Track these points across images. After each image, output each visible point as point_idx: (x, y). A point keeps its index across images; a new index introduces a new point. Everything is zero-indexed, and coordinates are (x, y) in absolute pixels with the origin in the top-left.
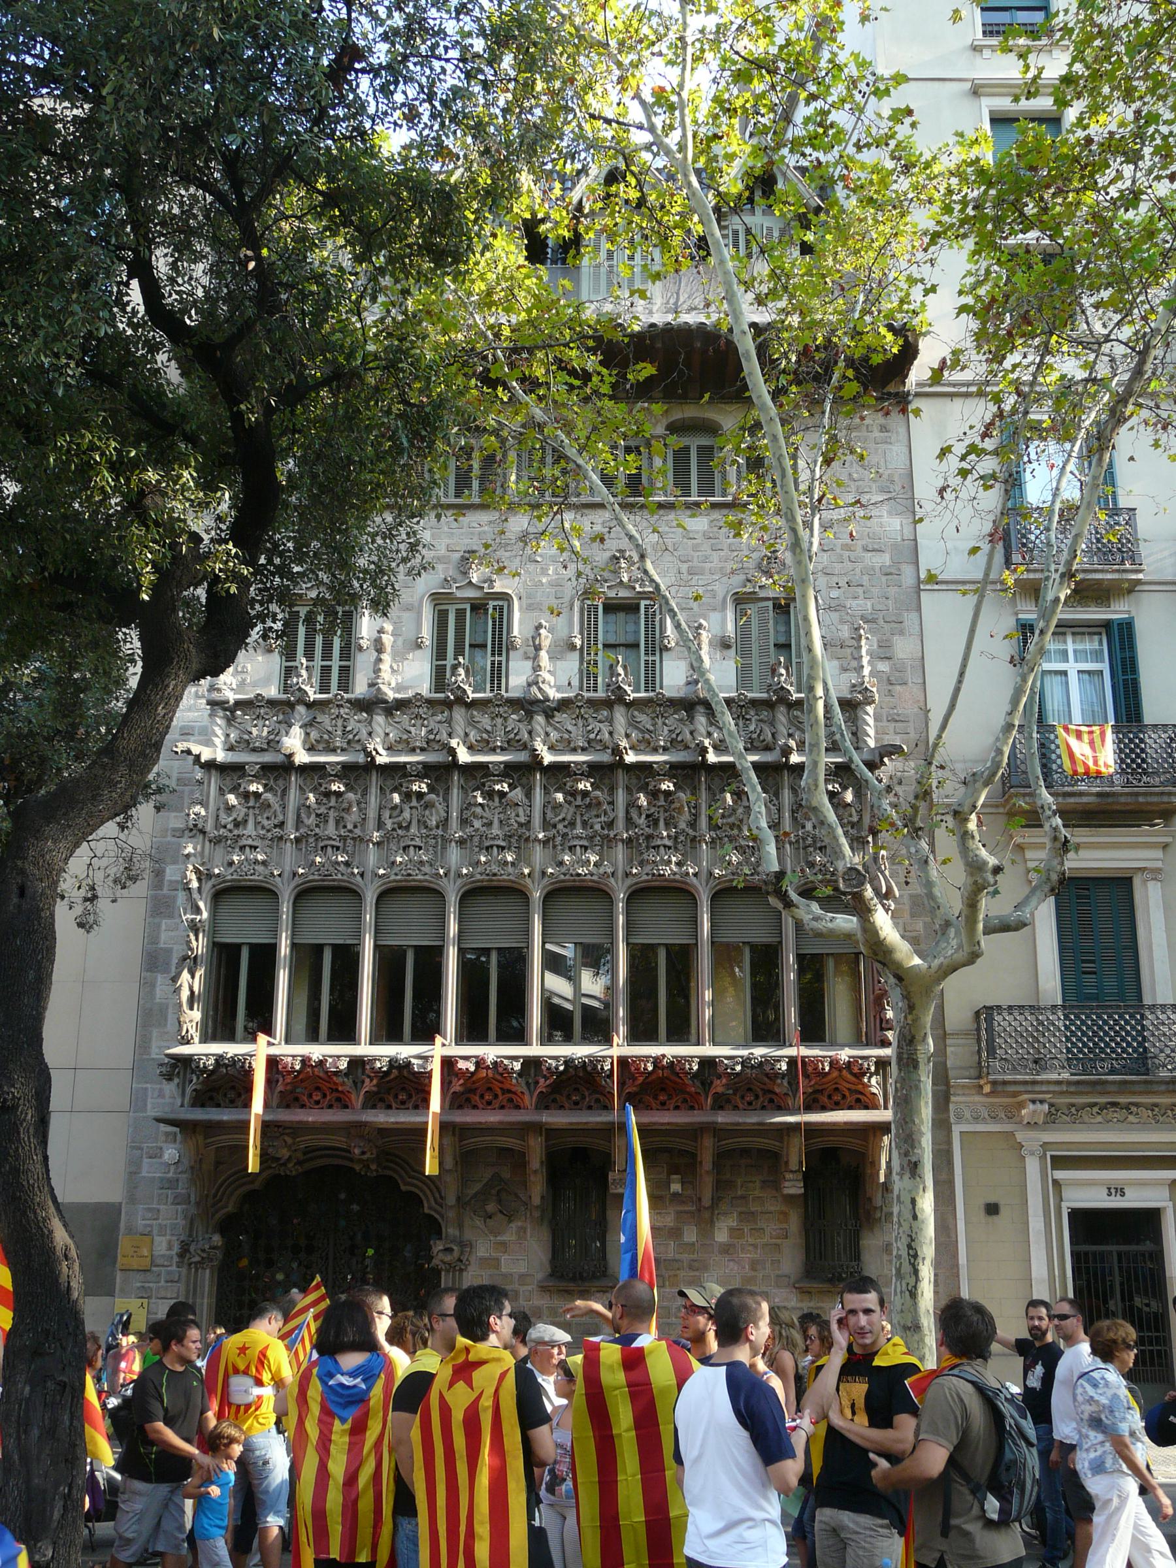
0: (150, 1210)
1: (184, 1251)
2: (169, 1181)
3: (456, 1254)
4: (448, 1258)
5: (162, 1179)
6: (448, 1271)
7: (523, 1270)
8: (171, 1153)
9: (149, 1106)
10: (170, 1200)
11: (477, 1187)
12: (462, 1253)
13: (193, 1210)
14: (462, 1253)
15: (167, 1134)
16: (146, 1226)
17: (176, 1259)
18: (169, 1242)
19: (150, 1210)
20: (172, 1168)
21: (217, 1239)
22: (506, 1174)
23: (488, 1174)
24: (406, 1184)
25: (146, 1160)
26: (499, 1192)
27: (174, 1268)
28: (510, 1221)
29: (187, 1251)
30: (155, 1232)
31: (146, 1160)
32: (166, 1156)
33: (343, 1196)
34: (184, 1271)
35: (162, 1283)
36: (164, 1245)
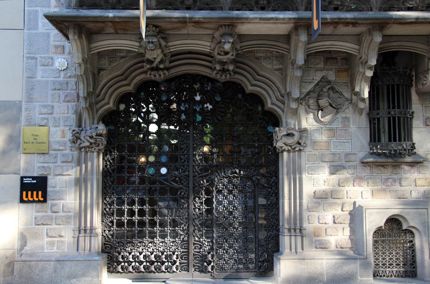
0: (45, 106)
1: (76, 138)
2: (60, 83)
3: (296, 138)
4: (290, 141)
5: (54, 83)
6: (289, 151)
7: (348, 151)
8: (60, 62)
9: (40, 24)
10: (62, 97)
11: (310, 87)
12: (301, 138)
13: (83, 104)
14: (301, 138)
15: (56, 47)
16: (43, 119)
17: (69, 144)
18: (63, 131)
19: (45, 106)
20: (62, 74)
21: (102, 128)
22: (331, 76)
23: (318, 77)
24: (252, 85)
25: (40, 68)
26: (329, 89)
27: (68, 151)
28: (337, 112)
29: (78, 138)
30: (51, 124)
31: (40, 68)
32: (57, 65)
33: (198, 98)
34: (76, 153)
35: (59, 163)
36: (59, 134)
